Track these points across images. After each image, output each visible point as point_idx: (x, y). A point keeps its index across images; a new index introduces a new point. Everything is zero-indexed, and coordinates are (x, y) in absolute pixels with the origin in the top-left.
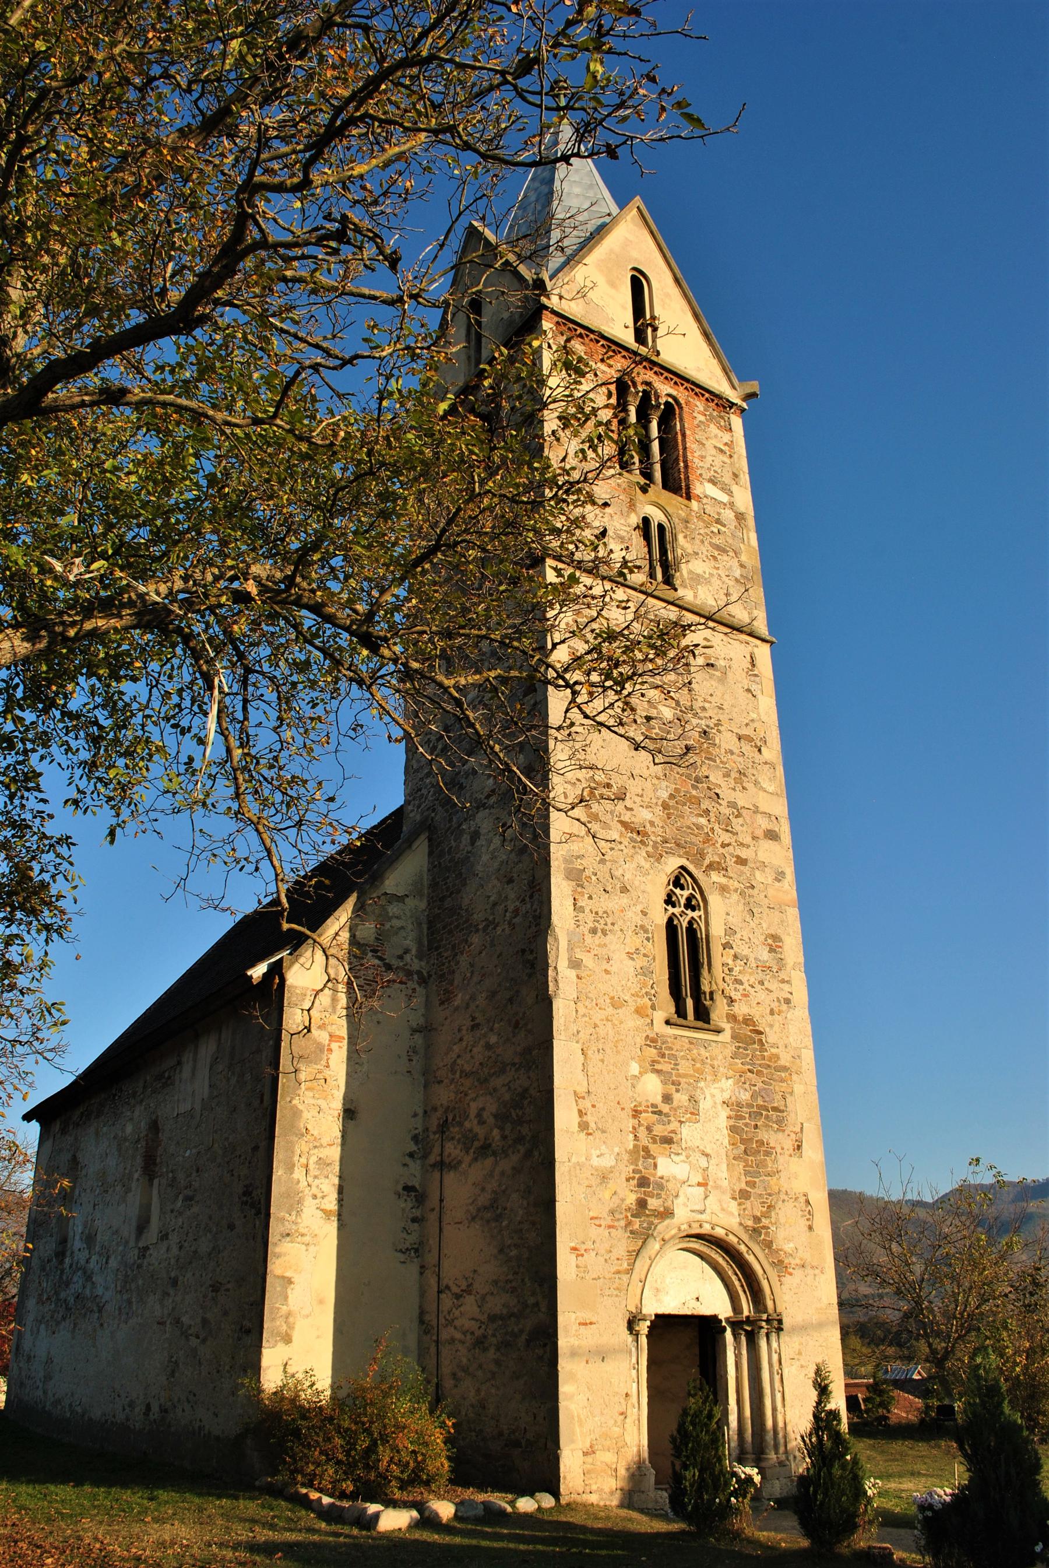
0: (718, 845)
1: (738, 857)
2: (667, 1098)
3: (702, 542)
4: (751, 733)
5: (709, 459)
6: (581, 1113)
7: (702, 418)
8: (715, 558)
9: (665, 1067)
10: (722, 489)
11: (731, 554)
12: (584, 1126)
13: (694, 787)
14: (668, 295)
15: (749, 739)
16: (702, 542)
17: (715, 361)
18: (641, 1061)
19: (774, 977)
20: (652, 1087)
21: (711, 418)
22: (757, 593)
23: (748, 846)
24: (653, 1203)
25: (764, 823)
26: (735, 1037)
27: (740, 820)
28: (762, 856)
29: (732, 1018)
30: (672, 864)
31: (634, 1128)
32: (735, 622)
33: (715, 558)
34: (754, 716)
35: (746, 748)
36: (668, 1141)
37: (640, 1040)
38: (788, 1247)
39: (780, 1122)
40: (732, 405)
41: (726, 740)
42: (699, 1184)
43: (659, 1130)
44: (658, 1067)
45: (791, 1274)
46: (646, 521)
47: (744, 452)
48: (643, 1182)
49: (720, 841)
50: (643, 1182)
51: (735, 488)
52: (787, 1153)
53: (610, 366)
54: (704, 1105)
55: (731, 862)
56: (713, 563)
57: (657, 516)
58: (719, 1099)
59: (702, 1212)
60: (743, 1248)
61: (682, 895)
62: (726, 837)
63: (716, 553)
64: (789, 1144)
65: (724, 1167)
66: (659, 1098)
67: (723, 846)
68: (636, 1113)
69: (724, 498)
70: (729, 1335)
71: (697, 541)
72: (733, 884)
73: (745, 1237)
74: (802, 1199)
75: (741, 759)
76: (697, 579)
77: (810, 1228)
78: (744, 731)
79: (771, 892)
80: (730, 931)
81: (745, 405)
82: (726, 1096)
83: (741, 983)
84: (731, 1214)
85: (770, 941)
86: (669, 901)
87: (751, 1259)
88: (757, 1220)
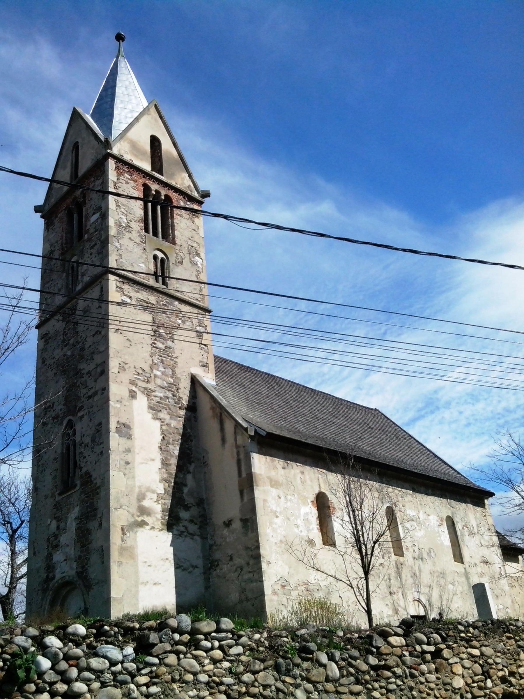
0: (82, 398)
2: (58, 528)
6: (34, 549)
7: (93, 184)
13: (76, 378)
19: (98, 444)
20: (54, 524)
21: (97, 179)
26: (82, 485)
31: (48, 546)
36: (57, 546)
38: (93, 577)
42: (65, 560)
43: (54, 543)
44: (56, 516)
45: (93, 589)
49: (82, 395)
52: (96, 529)
58: (74, 518)
59: (64, 573)
65: (73, 548)
66: (56, 529)
74: (100, 550)
77: (103, 562)
80: (82, 436)
82: (76, 515)
83: (85, 457)
85: (97, 428)
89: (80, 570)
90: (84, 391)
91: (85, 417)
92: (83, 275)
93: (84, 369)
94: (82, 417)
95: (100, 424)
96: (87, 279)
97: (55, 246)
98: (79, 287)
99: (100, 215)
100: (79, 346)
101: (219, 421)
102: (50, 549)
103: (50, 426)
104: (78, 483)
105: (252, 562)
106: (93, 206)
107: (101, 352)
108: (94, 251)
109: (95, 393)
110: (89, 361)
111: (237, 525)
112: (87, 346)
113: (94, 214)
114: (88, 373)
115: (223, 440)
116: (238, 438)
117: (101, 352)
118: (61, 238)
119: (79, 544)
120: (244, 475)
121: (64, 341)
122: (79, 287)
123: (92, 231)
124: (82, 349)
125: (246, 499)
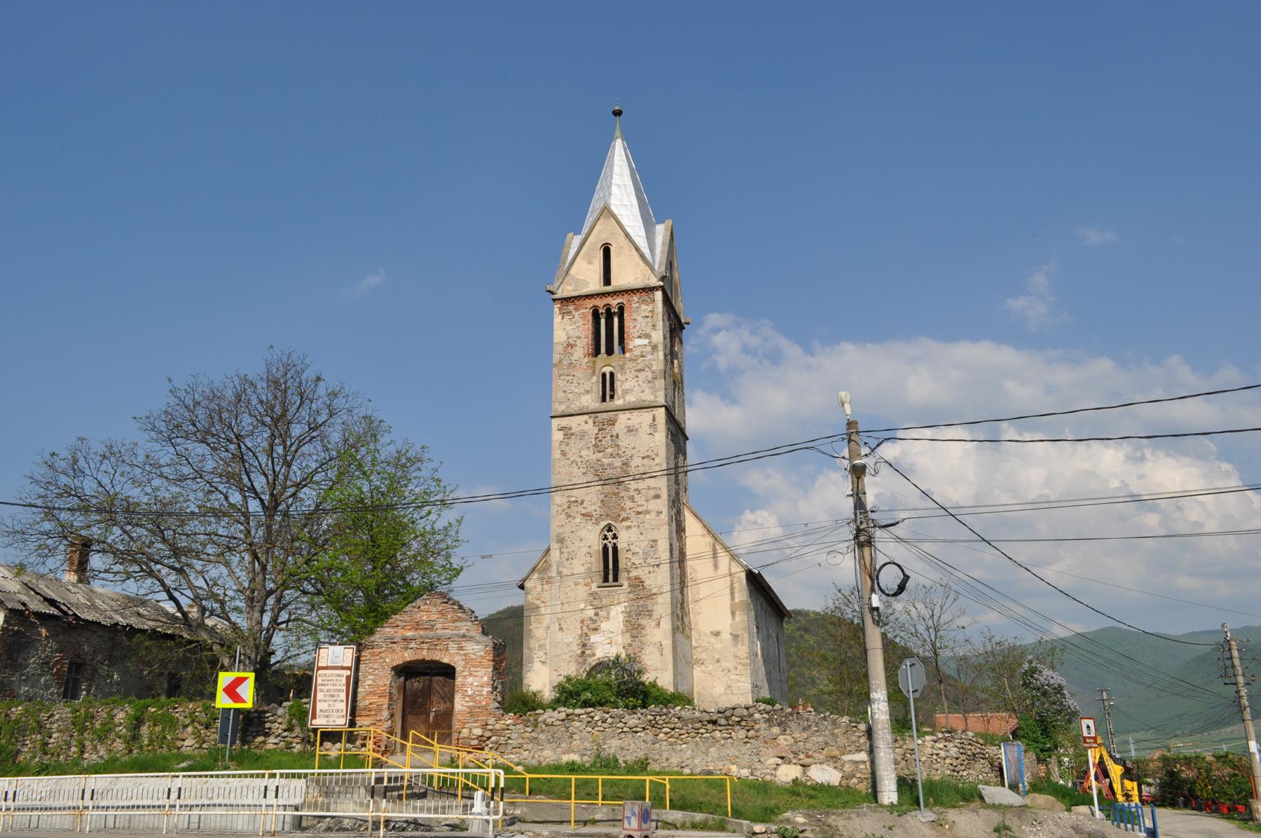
2: (596, 614)
4: (649, 453)
9: (596, 603)
12: (561, 629)
18: (585, 601)
20: (590, 612)
24: (587, 652)
25: (652, 493)
29: (629, 579)
30: (603, 524)
32: (646, 404)
35: (646, 461)
36: (595, 629)
37: (585, 594)
39: (650, 616)
41: (636, 462)
43: (592, 626)
46: (604, 375)
48: (584, 645)
50: (584, 645)
51: (653, 334)
54: (613, 614)
55: (633, 515)
57: (607, 370)
61: (610, 535)
62: (631, 505)
64: (653, 624)
68: (582, 621)
69: (645, 341)
86: (606, 538)
90: (629, 504)
92: (625, 392)
94: (628, 527)
95: (655, 541)
96: (631, 399)
98: (618, 402)
102: (585, 629)
103: (578, 520)
104: (626, 584)
105: (740, 667)
108: (642, 375)
109: (648, 512)
111: (726, 636)
112: (633, 464)
115: (716, 566)
118: (587, 337)
119: (628, 635)
120: (737, 600)
121: (596, 446)
122: (618, 402)
123: (637, 353)
125: (737, 619)
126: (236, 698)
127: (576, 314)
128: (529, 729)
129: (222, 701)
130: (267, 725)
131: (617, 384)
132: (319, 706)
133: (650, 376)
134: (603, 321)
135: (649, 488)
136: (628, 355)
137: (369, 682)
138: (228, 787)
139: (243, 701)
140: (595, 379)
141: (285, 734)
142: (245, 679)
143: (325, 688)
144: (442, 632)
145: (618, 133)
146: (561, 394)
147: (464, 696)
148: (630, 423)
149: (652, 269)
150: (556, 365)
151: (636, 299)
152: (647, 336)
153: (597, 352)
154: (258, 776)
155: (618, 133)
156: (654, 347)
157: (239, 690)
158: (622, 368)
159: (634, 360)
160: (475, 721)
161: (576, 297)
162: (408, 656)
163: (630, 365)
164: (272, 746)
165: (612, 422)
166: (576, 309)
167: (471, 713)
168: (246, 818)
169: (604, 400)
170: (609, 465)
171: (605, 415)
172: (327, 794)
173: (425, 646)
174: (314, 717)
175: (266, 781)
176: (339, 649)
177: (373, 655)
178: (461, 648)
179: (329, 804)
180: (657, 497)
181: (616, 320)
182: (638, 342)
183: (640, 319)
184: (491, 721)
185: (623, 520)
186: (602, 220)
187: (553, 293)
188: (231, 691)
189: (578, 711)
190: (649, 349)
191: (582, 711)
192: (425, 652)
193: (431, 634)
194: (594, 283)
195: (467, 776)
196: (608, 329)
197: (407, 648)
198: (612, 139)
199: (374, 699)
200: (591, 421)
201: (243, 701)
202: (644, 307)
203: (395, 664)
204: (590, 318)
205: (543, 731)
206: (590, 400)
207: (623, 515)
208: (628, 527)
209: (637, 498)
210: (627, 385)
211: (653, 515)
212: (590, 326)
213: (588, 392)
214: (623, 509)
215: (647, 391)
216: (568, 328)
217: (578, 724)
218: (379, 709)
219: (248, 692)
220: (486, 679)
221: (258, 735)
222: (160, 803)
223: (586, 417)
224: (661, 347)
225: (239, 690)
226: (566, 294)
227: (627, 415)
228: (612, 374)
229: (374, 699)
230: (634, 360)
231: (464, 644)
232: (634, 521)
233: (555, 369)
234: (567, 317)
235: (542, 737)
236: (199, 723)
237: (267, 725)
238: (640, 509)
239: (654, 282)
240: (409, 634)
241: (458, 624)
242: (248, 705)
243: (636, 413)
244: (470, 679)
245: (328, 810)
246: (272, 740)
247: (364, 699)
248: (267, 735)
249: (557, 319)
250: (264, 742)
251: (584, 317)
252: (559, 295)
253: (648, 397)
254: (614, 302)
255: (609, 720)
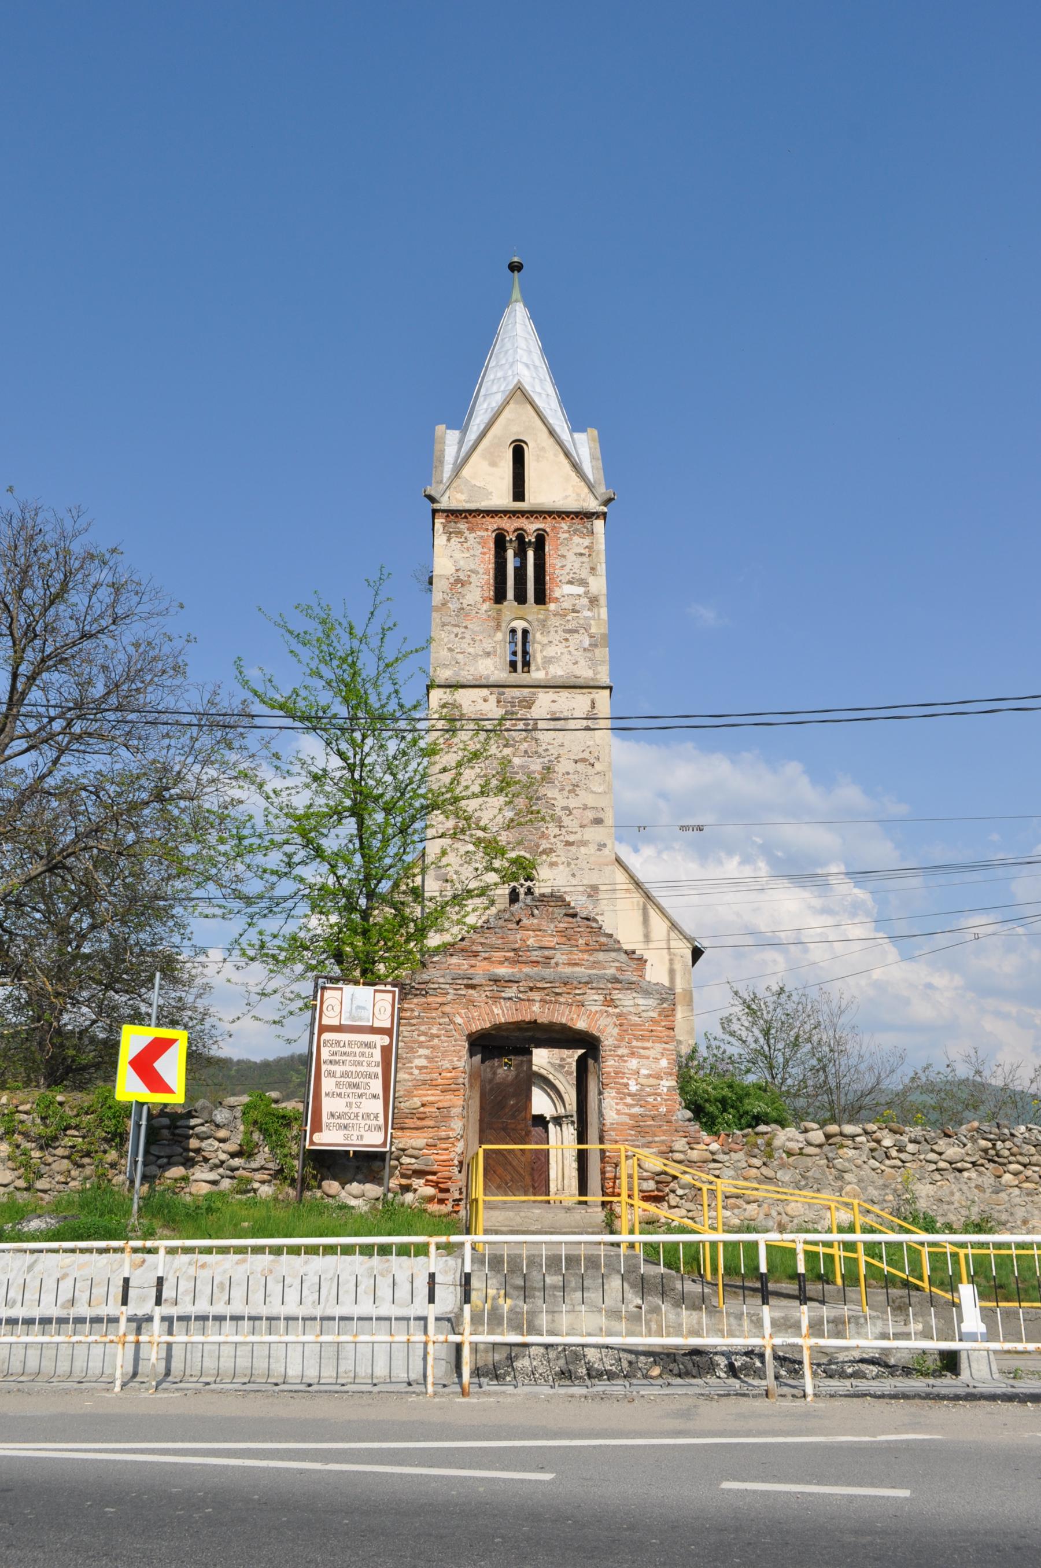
1: (567, 842)
3: (556, 632)
4: (586, 755)
5: (569, 566)
7: (567, 535)
8: (567, 640)
10: (580, 585)
11: (582, 631)
14: (543, 449)
15: (584, 760)
16: (556, 632)
17: (583, 483)
21: (576, 531)
22: (602, 653)
23: (576, 833)
25: (590, 815)
27: (571, 817)
28: (586, 838)
32: (581, 682)
33: (567, 640)
34: (591, 743)
35: (580, 766)
40: (593, 514)
41: (564, 766)
46: (513, 631)
47: (603, 547)
51: (591, 580)
53: (487, 530)
55: (560, 846)
56: (564, 643)
57: (519, 625)
60: (551, 1077)
62: (557, 831)
63: (568, 636)
67: (555, 837)
69: (581, 590)
70: (551, 1126)
71: (552, 633)
72: (559, 860)
73: (552, 1070)
75: (576, 776)
76: (548, 661)
78: (581, 756)
79: (592, 859)
81: (605, 509)
84: (543, 1057)
87: (556, 1082)
88: (562, 1059)
89: (558, 1062)
90: (553, 830)
91: (561, 867)
92: (548, 661)
93: (555, 799)
96: (557, 671)
97: (469, 576)
98: (537, 675)
99: (586, 593)
100: (542, 760)
101: (641, 911)
106: (567, 569)
107: (592, 792)
109: (584, 843)
110: (565, 793)
113: (570, 582)
114: (564, 808)
116: (673, 944)
117: (592, 792)
118: (486, 573)
122: (537, 675)
123: (567, 604)
124: (548, 769)
126: (155, 1082)
127: (471, 536)
128: (757, 1162)
129: (128, 1087)
130: (194, 1143)
131: (535, 649)
132: (328, 1105)
133: (587, 642)
134: (510, 554)
135: (585, 808)
136: (552, 606)
137: (423, 1062)
138: (204, 1274)
139: (168, 1090)
140: (499, 636)
141: (237, 1162)
142: (171, 1042)
143: (338, 1069)
144: (568, 970)
145: (516, 294)
146: (444, 653)
147: (623, 1092)
148: (555, 707)
149: (590, 487)
150: (437, 609)
151: (564, 525)
152: (583, 583)
153: (500, 596)
154: (404, 1251)
155: (516, 294)
156: (594, 601)
157: (158, 1065)
158: (543, 623)
159: (562, 615)
160: (648, 1145)
161: (470, 512)
162: (502, 1013)
163: (554, 621)
164: (205, 1188)
165: (529, 704)
166: (471, 530)
167: (640, 1130)
168: (312, 1350)
169: (513, 665)
170: (522, 767)
171: (516, 692)
172: (525, 1292)
173: (536, 996)
174: (317, 1127)
175: (434, 1262)
176: (363, 993)
177: (428, 1008)
178: (610, 1002)
179: (533, 1314)
180: (598, 821)
181: (530, 554)
182: (568, 589)
183: (571, 556)
184: (680, 1144)
185: (544, 852)
186: (512, 405)
187: (432, 499)
188: (145, 1065)
189: (849, 1129)
190: (585, 601)
191: (858, 1129)
192: (536, 1008)
193: (547, 972)
194: (501, 497)
195: (872, 1249)
196: (521, 567)
197: (496, 999)
198: (506, 302)
199: (432, 1096)
200: (493, 699)
201: (168, 1090)
202: (576, 539)
203: (476, 1027)
204: (492, 545)
205: (782, 1166)
206: (494, 669)
207: (544, 845)
208: (553, 864)
209: (566, 821)
210: (550, 651)
211: (592, 849)
212: (491, 556)
213: (488, 654)
214: (543, 836)
215: (582, 662)
216: (458, 555)
217: (851, 1153)
218: (444, 1114)
219: (173, 1067)
220: (664, 1063)
221: (170, 1164)
222: (103, 1311)
223: (485, 692)
224: (603, 601)
225: (158, 1065)
226: (454, 505)
227: (551, 694)
228: (525, 632)
229: (432, 1096)
230: (562, 615)
231: (616, 995)
232: (562, 854)
233: (434, 614)
234: (455, 540)
235: (784, 1176)
236: (25, 1135)
237: (194, 1143)
238: (571, 838)
239: (593, 505)
240: (503, 971)
241: (601, 956)
242: (177, 1097)
243: (565, 693)
244: (633, 1063)
245: (533, 1330)
246: (201, 1173)
247: (409, 1094)
248: (189, 1163)
249: (440, 540)
250: (185, 1179)
251: (483, 542)
252: (444, 504)
253: (585, 673)
254: (531, 527)
255: (911, 1148)
